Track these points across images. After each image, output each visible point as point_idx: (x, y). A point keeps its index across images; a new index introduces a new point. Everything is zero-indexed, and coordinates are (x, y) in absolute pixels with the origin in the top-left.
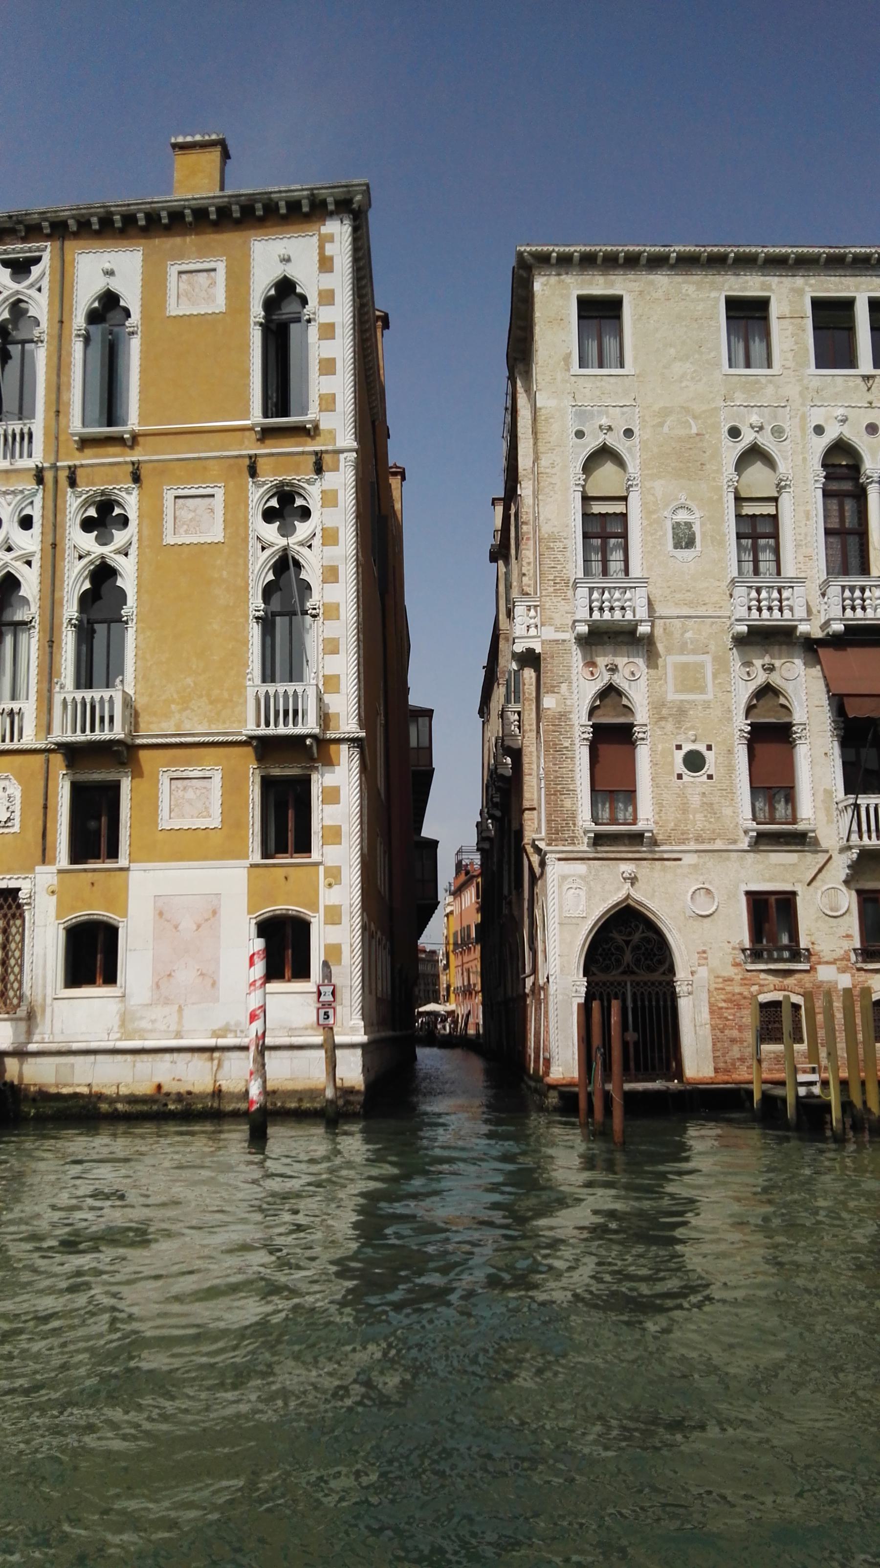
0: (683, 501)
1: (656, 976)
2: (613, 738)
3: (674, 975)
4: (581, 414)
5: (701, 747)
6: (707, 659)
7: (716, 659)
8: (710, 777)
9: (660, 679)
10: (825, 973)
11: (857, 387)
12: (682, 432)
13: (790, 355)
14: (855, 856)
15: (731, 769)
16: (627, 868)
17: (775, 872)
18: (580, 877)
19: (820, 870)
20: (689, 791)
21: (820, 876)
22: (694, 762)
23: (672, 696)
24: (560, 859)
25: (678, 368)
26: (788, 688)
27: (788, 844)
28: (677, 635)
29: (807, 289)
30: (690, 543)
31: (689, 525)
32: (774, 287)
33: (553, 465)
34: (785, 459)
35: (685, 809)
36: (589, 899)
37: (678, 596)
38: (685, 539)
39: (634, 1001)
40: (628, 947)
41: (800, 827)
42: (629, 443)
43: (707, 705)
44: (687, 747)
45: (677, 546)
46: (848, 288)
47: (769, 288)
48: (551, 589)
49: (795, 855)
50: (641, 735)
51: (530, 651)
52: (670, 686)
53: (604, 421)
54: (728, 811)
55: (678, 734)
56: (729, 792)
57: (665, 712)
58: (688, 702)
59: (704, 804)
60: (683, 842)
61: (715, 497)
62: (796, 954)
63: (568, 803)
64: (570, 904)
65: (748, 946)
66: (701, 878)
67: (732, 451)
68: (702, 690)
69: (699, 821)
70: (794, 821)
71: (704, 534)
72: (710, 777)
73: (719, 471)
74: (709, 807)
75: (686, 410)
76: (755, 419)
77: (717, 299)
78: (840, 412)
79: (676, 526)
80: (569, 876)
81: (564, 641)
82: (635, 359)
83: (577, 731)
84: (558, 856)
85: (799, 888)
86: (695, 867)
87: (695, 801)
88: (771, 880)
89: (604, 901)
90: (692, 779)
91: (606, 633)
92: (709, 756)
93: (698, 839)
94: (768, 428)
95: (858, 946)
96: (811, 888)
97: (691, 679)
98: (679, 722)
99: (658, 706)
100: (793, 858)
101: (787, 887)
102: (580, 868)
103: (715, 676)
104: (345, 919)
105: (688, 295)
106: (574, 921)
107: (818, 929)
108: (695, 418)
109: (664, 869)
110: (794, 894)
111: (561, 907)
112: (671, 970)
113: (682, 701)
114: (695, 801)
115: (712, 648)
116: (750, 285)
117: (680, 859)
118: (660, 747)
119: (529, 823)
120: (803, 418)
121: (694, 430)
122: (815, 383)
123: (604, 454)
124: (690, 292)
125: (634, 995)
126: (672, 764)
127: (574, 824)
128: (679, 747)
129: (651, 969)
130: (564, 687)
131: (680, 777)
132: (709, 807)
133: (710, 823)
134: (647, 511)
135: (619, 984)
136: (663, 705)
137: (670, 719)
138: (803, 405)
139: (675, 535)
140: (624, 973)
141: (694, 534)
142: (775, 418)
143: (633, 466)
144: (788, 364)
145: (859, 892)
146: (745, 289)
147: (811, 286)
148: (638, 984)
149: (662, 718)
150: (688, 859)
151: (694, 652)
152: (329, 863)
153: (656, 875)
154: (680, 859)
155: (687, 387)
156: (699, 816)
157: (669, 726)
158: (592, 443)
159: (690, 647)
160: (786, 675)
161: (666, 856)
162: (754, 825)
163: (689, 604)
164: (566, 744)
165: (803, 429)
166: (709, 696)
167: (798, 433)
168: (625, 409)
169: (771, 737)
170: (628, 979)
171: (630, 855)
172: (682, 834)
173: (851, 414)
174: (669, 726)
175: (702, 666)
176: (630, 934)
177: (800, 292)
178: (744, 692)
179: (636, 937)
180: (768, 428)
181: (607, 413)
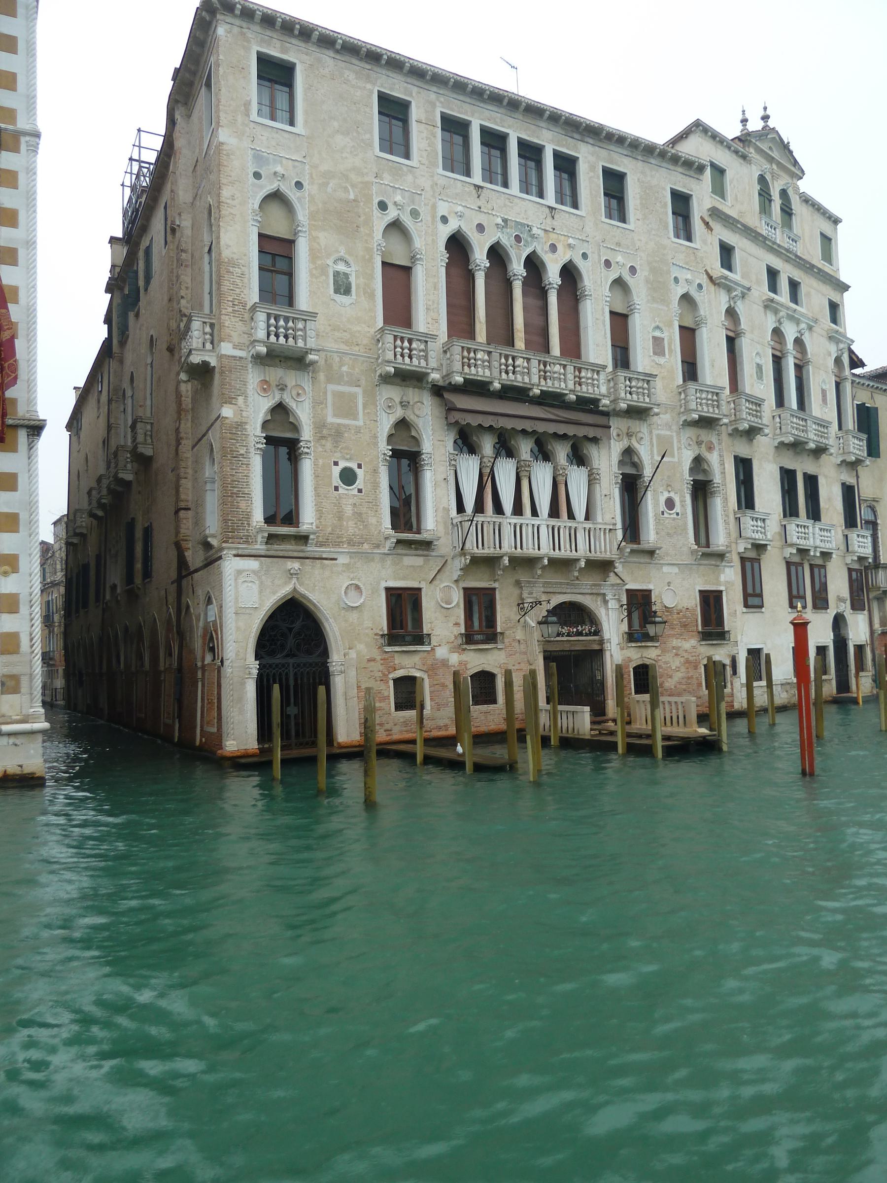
0: (342, 254)
1: (313, 659)
3: (328, 657)
4: (258, 157)
5: (354, 466)
6: (359, 391)
7: (365, 392)
8: (360, 491)
9: (322, 403)
10: (442, 652)
12: (341, 195)
13: (425, 154)
14: (468, 561)
15: (376, 486)
16: (295, 565)
17: (404, 573)
18: (254, 572)
19: (439, 571)
20: (344, 501)
21: (438, 577)
22: (348, 477)
23: (331, 419)
24: (235, 556)
25: (340, 140)
26: (420, 423)
27: (416, 549)
28: (335, 367)
29: (438, 104)
30: (347, 291)
31: (346, 275)
32: (414, 94)
33: (233, 198)
34: (420, 237)
36: (261, 592)
37: (337, 334)
38: (343, 287)
39: (296, 680)
40: (293, 635)
41: (424, 536)
42: (299, 194)
43: (358, 430)
44: (343, 464)
45: (337, 291)
46: (466, 113)
47: (411, 95)
48: (230, 309)
49: (422, 558)
50: (306, 450)
51: (205, 364)
52: (330, 411)
53: (279, 169)
54: (373, 520)
55: (335, 452)
56: (374, 504)
57: (325, 432)
58: (345, 426)
59: (354, 513)
60: (338, 544)
61: (367, 257)
62: (420, 639)
63: (243, 505)
64: (243, 596)
65: (386, 632)
66: (352, 576)
67: (380, 222)
68: (355, 418)
69: (351, 528)
70: (419, 532)
71: (358, 286)
72: (360, 491)
73: (370, 235)
74: (359, 516)
76: (398, 198)
77: (372, 92)
78: (460, 209)
79: (337, 274)
80: (244, 571)
81: (241, 358)
82: (306, 122)
83: (252, 440)
85: (423, 585)
86: (347, 566)
87: (348, 510)
88: (404, 578)
89: (274, 593)
90: (346, 492)
91: (278, 356)
92: (360, 473)
93: (350, 543)
95: (463, 631)
96: (432, 586)
97: (346, 407)
98: (337, 442)
99: (320, 426)
100: (419, 561)
101: (415, 585)
102: (253, 564)
103: (365, 406)
104: (24, 609)
105: (348, 80)
106: (248, 611)
107: (436, 619)
108: (353, 186)
109: (323, 567)
110: (420, 589)
111: (237, 599)
112: (325, 653)
113: (338, 424)
114: (348, 510)
115: (363, 382)
116: (398, 87)
117: (336, 559)
118: (321, 462)
119: (184, 521)
120: (434, 207)
121: (352, 197)
122: (442, 181)
123: (276, 197)
124: (350, 78)
125: (295, 674)
126: (330, 476)
127: (249, 524)
129: (309, 652)
130: (241, 400)
131: (336, 488)
132: (359, 516)
133: (359, 529)
134: (314, 255)
135: (283, 666)
136: (324, 426)
137: (329, 439)
138: (433, 196)
139: (336, 282)
140: (287, 656)
141: (350, 284)
142: (413, 202)
143: (302, 215)
144: (424, 161)
145: (464, 589)
146: (392, 89)
147: (441, 102)
148: (299, 665)
149: (323, 437)
150: (343, 560)
151: (350, 384)
153: (317, 572)
154: (336, 559)
155: (346, 158)
156: (351, 523)
157: (329, 445)
158: (269, 187)
159: (346, 379)
160: (417, 412)
161: (324, 556)
162: (392, 532)
163: (346, 343)
164: (242, 452)
165: (433, 217)
166: (360, 423)
167: (429, 219)
168: (296, 163)
170: (291, 661)
171: (296, 554)
172: (338, 538)
173: (467, 212)
174: (329, 445)
175: (354, 396)
176: (293, 622)
177: (434, 105)
178: (386, 424)
179: (298, 625)
181: (281, 163)
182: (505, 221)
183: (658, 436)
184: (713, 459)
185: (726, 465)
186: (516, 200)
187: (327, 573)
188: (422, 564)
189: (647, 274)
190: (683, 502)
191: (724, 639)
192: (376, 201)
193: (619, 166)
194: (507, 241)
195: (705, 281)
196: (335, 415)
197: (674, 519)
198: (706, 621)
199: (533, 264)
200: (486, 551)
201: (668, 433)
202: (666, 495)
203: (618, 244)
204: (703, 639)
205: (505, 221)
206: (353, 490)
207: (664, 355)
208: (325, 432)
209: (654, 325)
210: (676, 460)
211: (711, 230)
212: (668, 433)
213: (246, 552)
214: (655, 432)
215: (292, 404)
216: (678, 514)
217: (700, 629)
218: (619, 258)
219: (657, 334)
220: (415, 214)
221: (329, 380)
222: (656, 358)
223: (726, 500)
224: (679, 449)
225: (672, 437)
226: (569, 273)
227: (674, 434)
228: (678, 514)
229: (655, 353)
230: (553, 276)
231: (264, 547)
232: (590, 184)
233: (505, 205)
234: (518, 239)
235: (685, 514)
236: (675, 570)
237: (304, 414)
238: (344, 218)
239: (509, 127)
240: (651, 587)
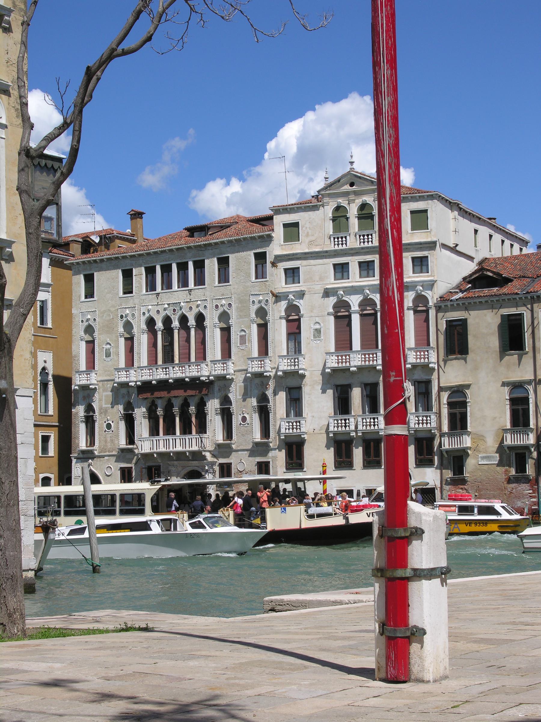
12: (108, 318)
15: (118, 428)
22: (109, 426)
23: (104, 406)
35: (106, 441)
52: (103, 402)
54: (116, 442)
56: (117, 436)
63: (77, 441)
69: (109, 445)
74: (112, 441)
75: (109, 310)
87: (109, 439)
99: (101, 409)
114: (109, 439)
121: (111, 317)
128: (105, 422)
144: (137, 292)
149: (101, 413)
163: (109, 375)
174: (103, 416)
187: (101, 463)
189: (237, 305)
190: (251, 418)
192: (119, 316)
194: (169, 313)
196: (105, 404)
199: (184, 319)
200: (160, 450)
203: (223, 295)
209: (240, 329)
216: (248, 424)
218: (224, 302)
223: (275, 413)
224: (251, 390)
227: (249, 384)
228: (248, 424)
230: (192, 322)
238: (109, 328)
239: (172, 260)
240: (231, 461)
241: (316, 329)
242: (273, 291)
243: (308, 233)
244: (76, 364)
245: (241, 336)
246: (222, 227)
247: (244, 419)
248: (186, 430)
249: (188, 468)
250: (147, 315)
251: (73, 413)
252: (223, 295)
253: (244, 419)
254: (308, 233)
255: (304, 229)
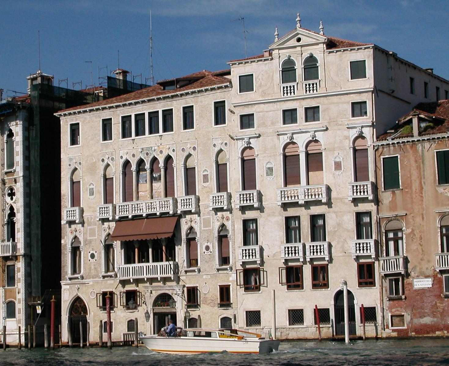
2: (75, 250)
7: (98, 227)
8: (96, 260)
11: (131, 143)
15: (100, 257)
22: (93, 256)
23: (88, 238)
24: (64, 285)
28: (90, 220)
29: (120, 114)
36: (69, 295)
42: (80, 166)
54: (99, 269)
56: (100, 264)
67: (102, 166)
69: (93, 272)
74: (95, 268)
78: (126, 151)
83: (68, 249)
84: (64, 283)
87: (93, 267)
93: (93, 278)
94: (110, 158)
99: (85, 241)
102: (68, 287)
109: (86, 286)
114: (93, 267)
128: (90, 252)
131: (89, 260)
146: (106, 117)
147: (121, 113)
149: (86, 244)
152: (19, 288)
164: (66, 253)
166: (96, 237)
169: (108, 248)
180: (110, 158)
182: (143, 149)
183: (204, 219)
184: (228, 225)
185: (235, 226)
186: (147, 138)
187: (87, 288)
188: (113, 283)
191: (230, 307)
193: (190, 104)
195: (228, 140)
196: (90, 237)
197: (209, 255)
198: (222, 299)
199: (154, 160)
201: (209, 216)
202: (206, 244)
204: (220, 307)
205: (143, 149)
206: (94, 260)
207: (208, 182)
208: (87, 243)
210: (212, 228)
211: (234, 113)
212: (209, 216)
213: (66, 283)
214: (202, 217)
215: (78, 236)
216: (211, 252)
217: (219, 302)
219: (205, 173)
220: (112, 159)
221: (88, 225)
222: (205, 185)
223: (234, 243)
225: (210, 218)
226: (168, 159)
228: (211, 252)
229: (204, 182)
231: (70, 281)
232: (178, 119)
233: (143, 142)
234: (147, 154)
235: (214, 251)
236: (209, 277)
237: (81, 239)
241: (269, 168)
242: (231, 135)
243: (261, 84)
244: (65, 202)
245: (204, 175)
246: (190, 81)
247: (207, 248)
248: (157, 259)
249: (159, 291)
250: (124, 159)
251: (62, 245)
252: (188, 139)
253: (207, 248)
254: (261, 84)
255: (257, 80)
